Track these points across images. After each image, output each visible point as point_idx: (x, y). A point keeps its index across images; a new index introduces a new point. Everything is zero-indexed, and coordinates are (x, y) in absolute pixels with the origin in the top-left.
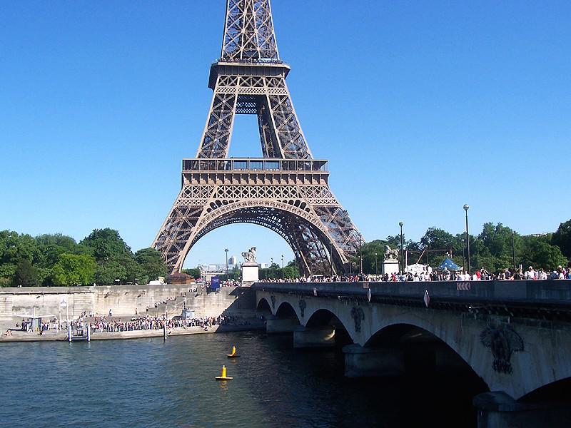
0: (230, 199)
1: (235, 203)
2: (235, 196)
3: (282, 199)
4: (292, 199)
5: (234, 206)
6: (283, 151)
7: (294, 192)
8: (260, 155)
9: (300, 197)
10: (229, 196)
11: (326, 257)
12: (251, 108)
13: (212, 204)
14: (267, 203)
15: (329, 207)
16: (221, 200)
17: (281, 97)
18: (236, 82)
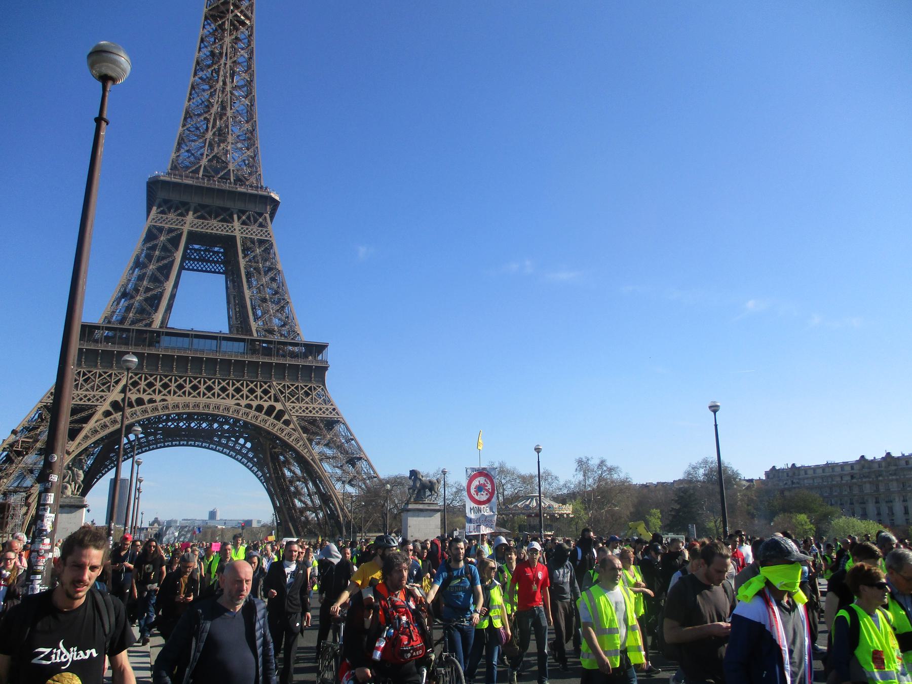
0: (149, 397)
2: (160, 392)
3: (244, 402)
4: (261, 403)
6: (254, 325)
10: (150, 391)
15: (322, 419)
17: (261, 242)
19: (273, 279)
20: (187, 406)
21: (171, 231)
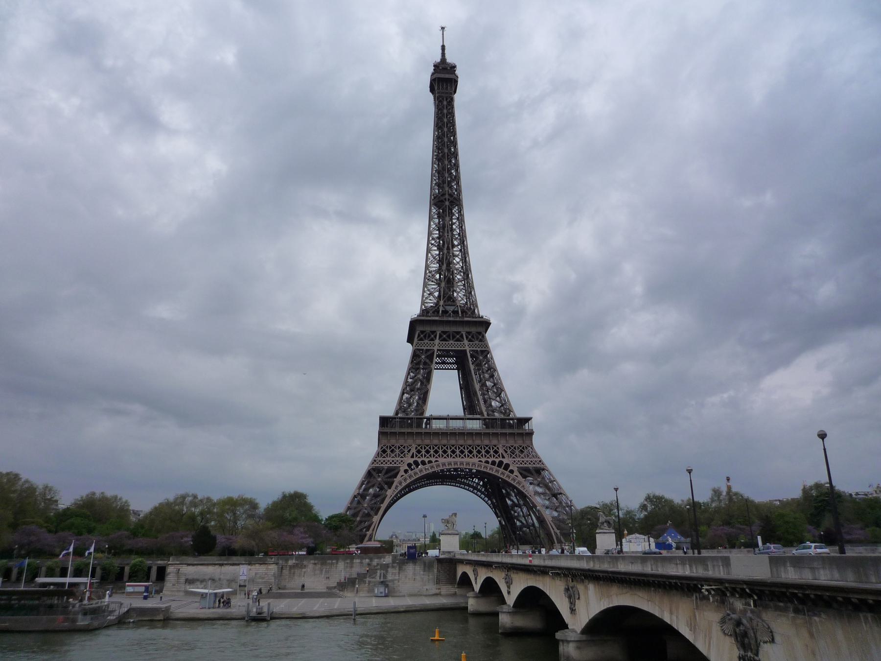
1: (434, 464)
3: (484, 460)
5: (432, 467)
7: (496, 452)
8: (460, 412)
9: (503, 457)
11: (533, 525)
12: (451, 363)
13: (409, 465)
14: (468, 464)
16: (419, 460)
17: (482, 352)
18: (435, 337)
19: (492, 376)
20: (450, 464)
21: (427, 350)
